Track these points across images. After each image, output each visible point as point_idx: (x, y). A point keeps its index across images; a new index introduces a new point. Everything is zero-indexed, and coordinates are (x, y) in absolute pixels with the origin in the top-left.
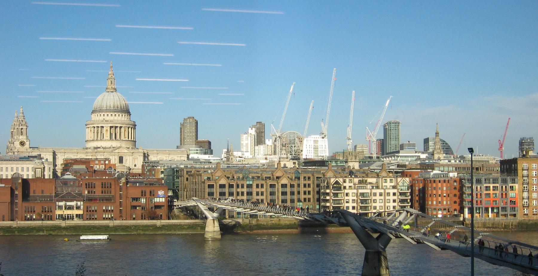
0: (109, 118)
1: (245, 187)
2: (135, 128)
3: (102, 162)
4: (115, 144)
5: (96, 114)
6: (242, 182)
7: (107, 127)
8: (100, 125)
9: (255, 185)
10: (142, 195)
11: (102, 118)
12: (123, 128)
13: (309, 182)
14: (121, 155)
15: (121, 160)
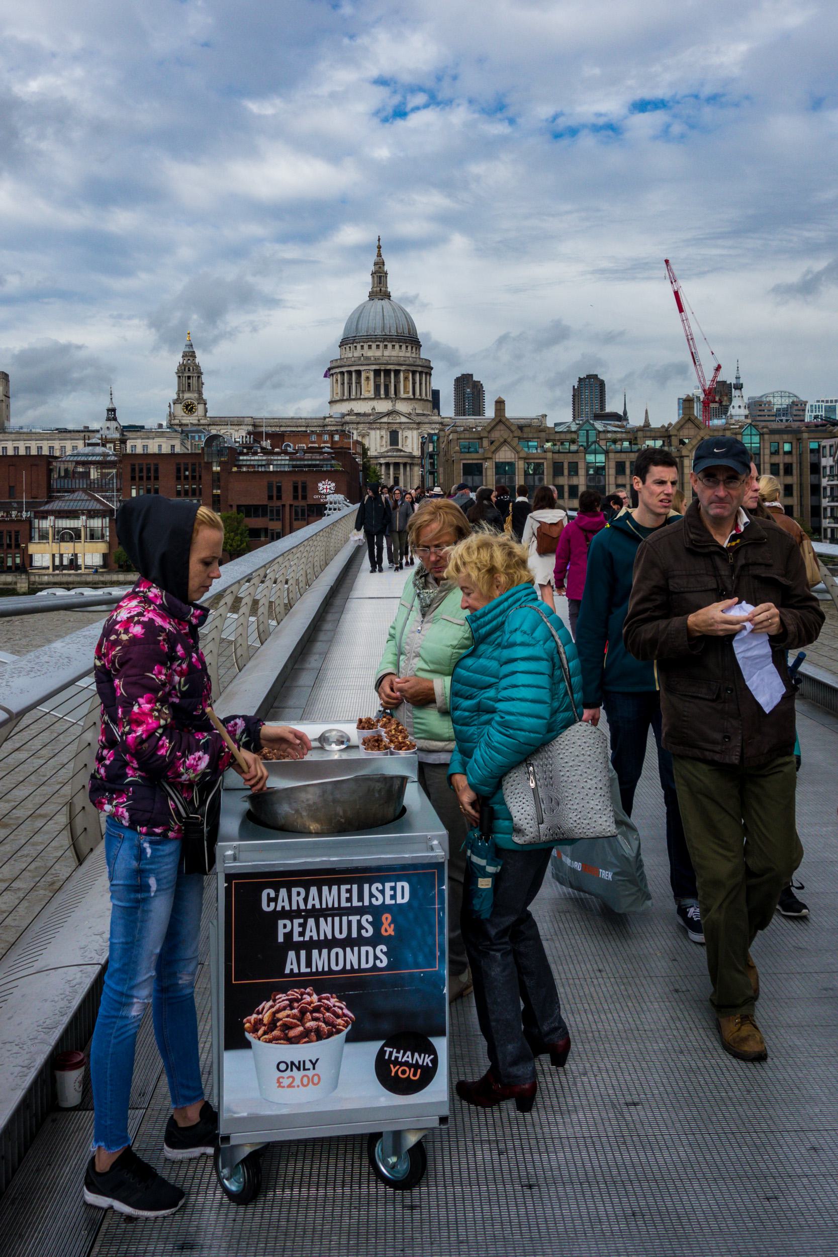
0: (373, 353)
1: (582, 472)
2: (430, 375)
3: (326, 437)
4: (383, 406)
5: (347, 347)
6: (571, 458)
7: (368, 371)
8: (353, 369)
9: (612, 464)
10: (270, 498)
11: (356, 354)
12: (402, 374)
13: (788, 459)
14: (394, 427)
15: (394, 438)
